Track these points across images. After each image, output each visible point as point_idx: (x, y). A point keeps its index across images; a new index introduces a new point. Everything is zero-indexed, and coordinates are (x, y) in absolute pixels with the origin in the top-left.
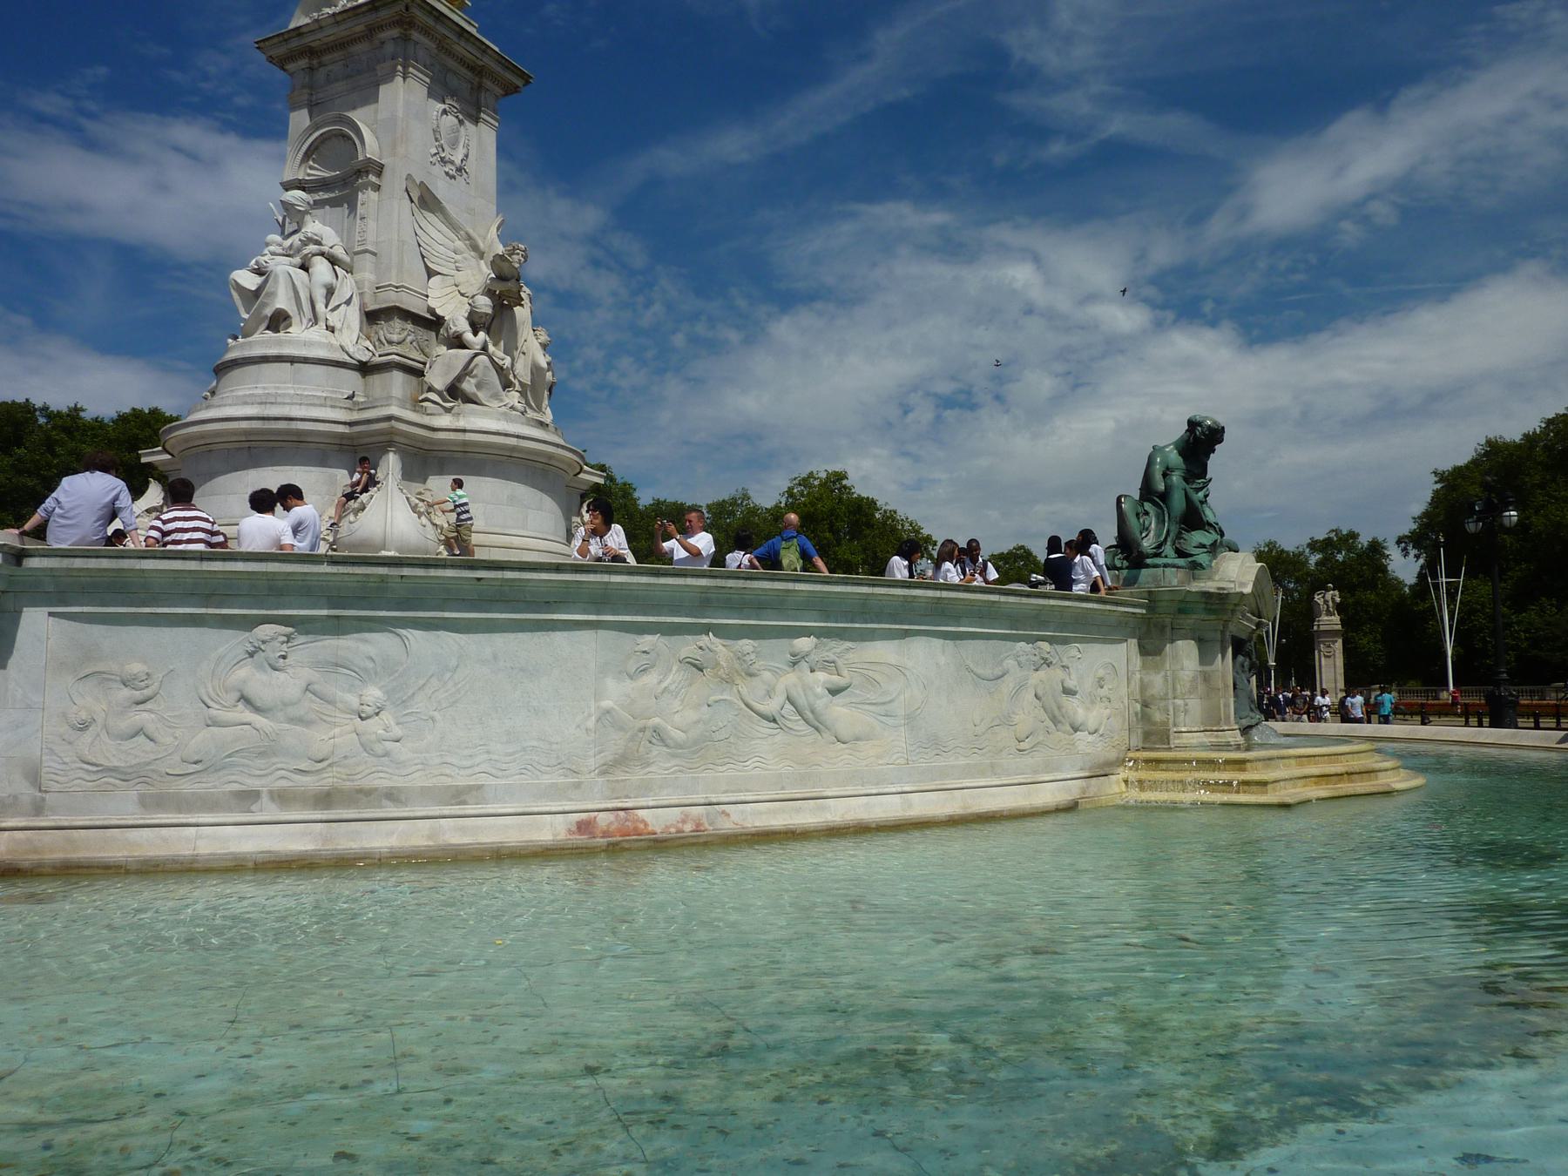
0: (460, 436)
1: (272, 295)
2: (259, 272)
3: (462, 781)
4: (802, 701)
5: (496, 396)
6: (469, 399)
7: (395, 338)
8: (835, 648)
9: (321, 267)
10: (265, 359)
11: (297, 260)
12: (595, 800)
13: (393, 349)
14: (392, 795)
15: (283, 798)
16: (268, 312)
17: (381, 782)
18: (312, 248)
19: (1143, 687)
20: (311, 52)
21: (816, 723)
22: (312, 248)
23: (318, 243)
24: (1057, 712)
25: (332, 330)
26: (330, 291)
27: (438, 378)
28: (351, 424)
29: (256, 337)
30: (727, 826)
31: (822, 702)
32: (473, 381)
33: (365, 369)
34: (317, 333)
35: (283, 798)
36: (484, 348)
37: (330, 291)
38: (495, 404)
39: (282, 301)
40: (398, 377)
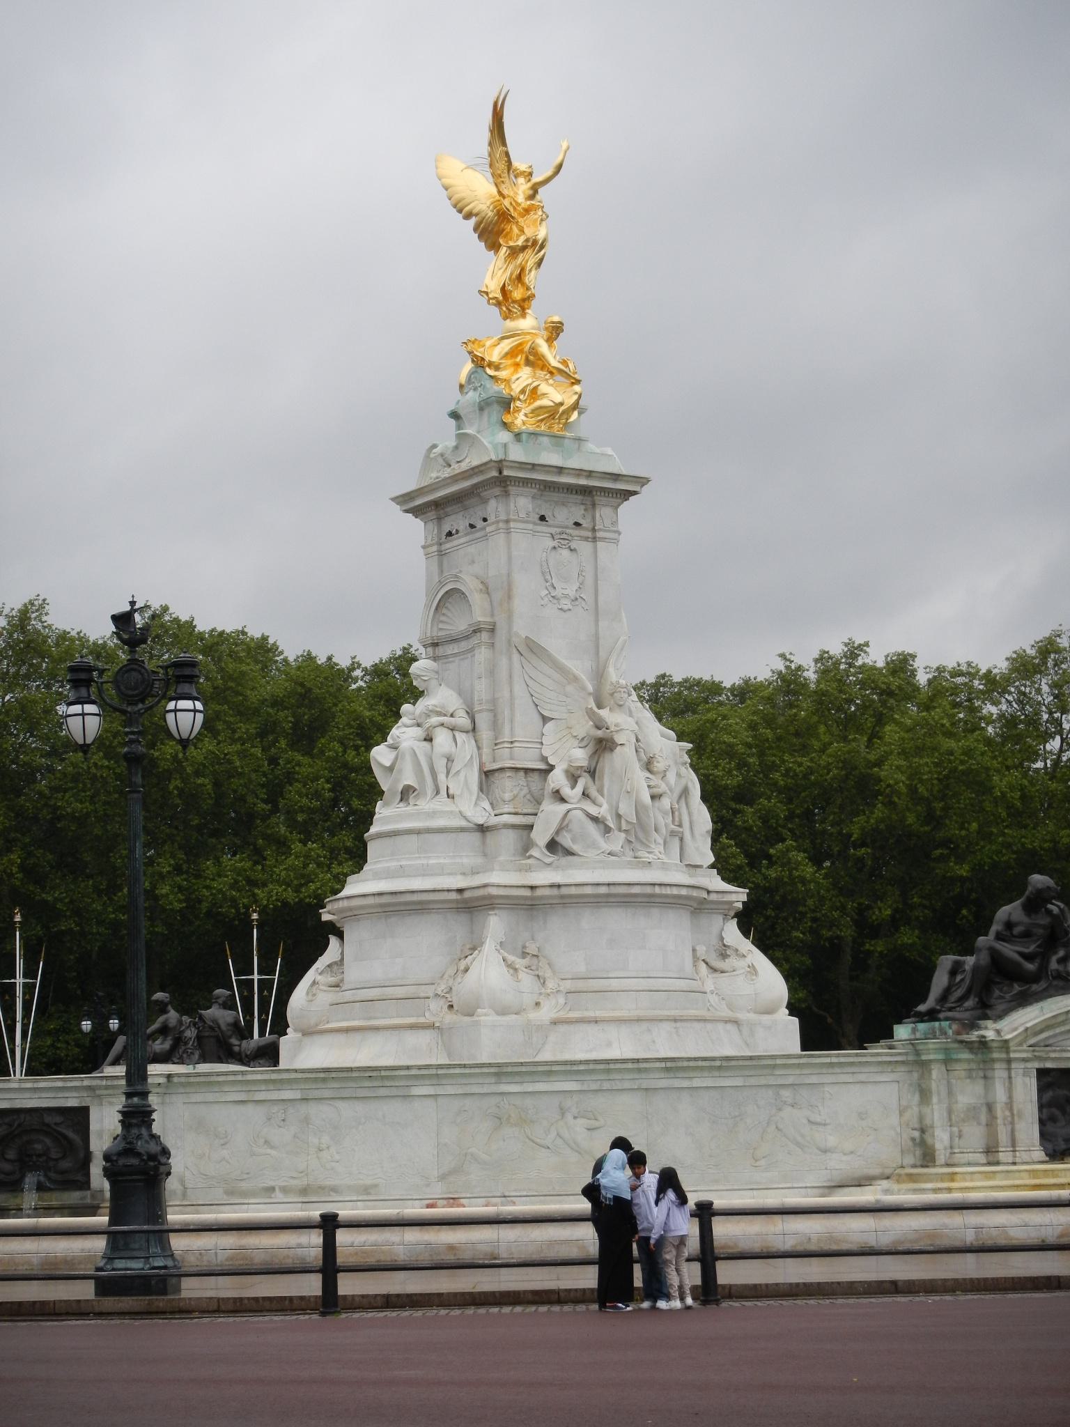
1: (400, 771)
2: (394, 747)
3: (368, 1182)
6: (569, 853)
12: (437, 1191)
14: (334, 1189)
15: (285, 1190)
17: (328, 1183)
18: (435, 720)
19: (921, 1118)
22: (435, 720)
24: (799, 1139)
26: (450, 759)
27: (541, 836)
33: (482, 829)
34: (441, 803)
35: (285, 1190)
37: (450, 759)
39: (409, 779)
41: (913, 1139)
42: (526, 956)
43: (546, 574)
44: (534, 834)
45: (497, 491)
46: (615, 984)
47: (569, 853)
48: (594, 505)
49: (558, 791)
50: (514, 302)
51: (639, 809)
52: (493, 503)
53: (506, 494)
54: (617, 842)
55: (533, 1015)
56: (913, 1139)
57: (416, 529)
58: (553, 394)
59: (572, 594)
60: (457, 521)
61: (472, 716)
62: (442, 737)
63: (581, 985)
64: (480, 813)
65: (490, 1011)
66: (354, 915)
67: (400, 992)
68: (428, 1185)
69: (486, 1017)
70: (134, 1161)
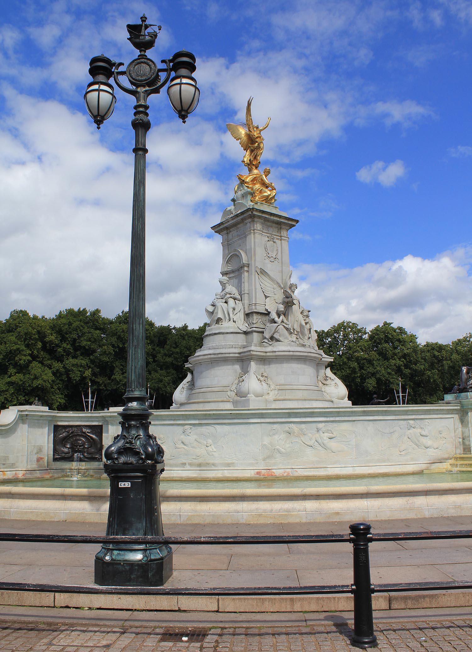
0: (274, 354)
1: (217, 313)
4: (320, 441)
5: (287, 338)
6: (278, 340)
7: (254, 322)
8: (330, 426)
9: (231, 301)
10: (215, 334)
11: (224, 301)
12: (261, 466)
13: (254, 326)
14: (214, 465)
15: (190, 464)
16: (216, 318)
17: (211, 461)
18: (228, 296)
20: (227, 228)
21: (325, 447)
22: (228, 296)
23: (230, 294)
24: (417, 443)
25: (234, 322)
26: (234, 309)
27: (267, 335)
28: (240, 353)
29: (213, 327)
30: (296, 474)
31: (326, 441)
32: (278, 334)
33: (245, 333)
35: (190, 464)
36: (282, 322)
37: (234, 309)
38: (286, 341)
39: (220, 315)
40: (255, 334)
41: (459, 442)
42: (263, 378)
43: (266, 249)
44: (265, 334)
45: (250, 220)
46: (295, 387)
47: (278, 340)
48: (281, 228)
49: (273, 319)
50: (253, 165)
51: (301, 326)
52: (248, 224)
53: (253, 221)
54: (294, 338)
55: (267, 397)
56: (459, 442)
57: (219, 238)
58: (267, 193)
59: (274, 257)
60: (234, 233)
61: (241, 295)
62: (231, 301)
63: (283, 387)
64: (244, 327)
65: (253, 395)
66: (200, 363)
67: (216, 389)
68: (257, 463)
69: (251, 396)
70: (132, 460)
